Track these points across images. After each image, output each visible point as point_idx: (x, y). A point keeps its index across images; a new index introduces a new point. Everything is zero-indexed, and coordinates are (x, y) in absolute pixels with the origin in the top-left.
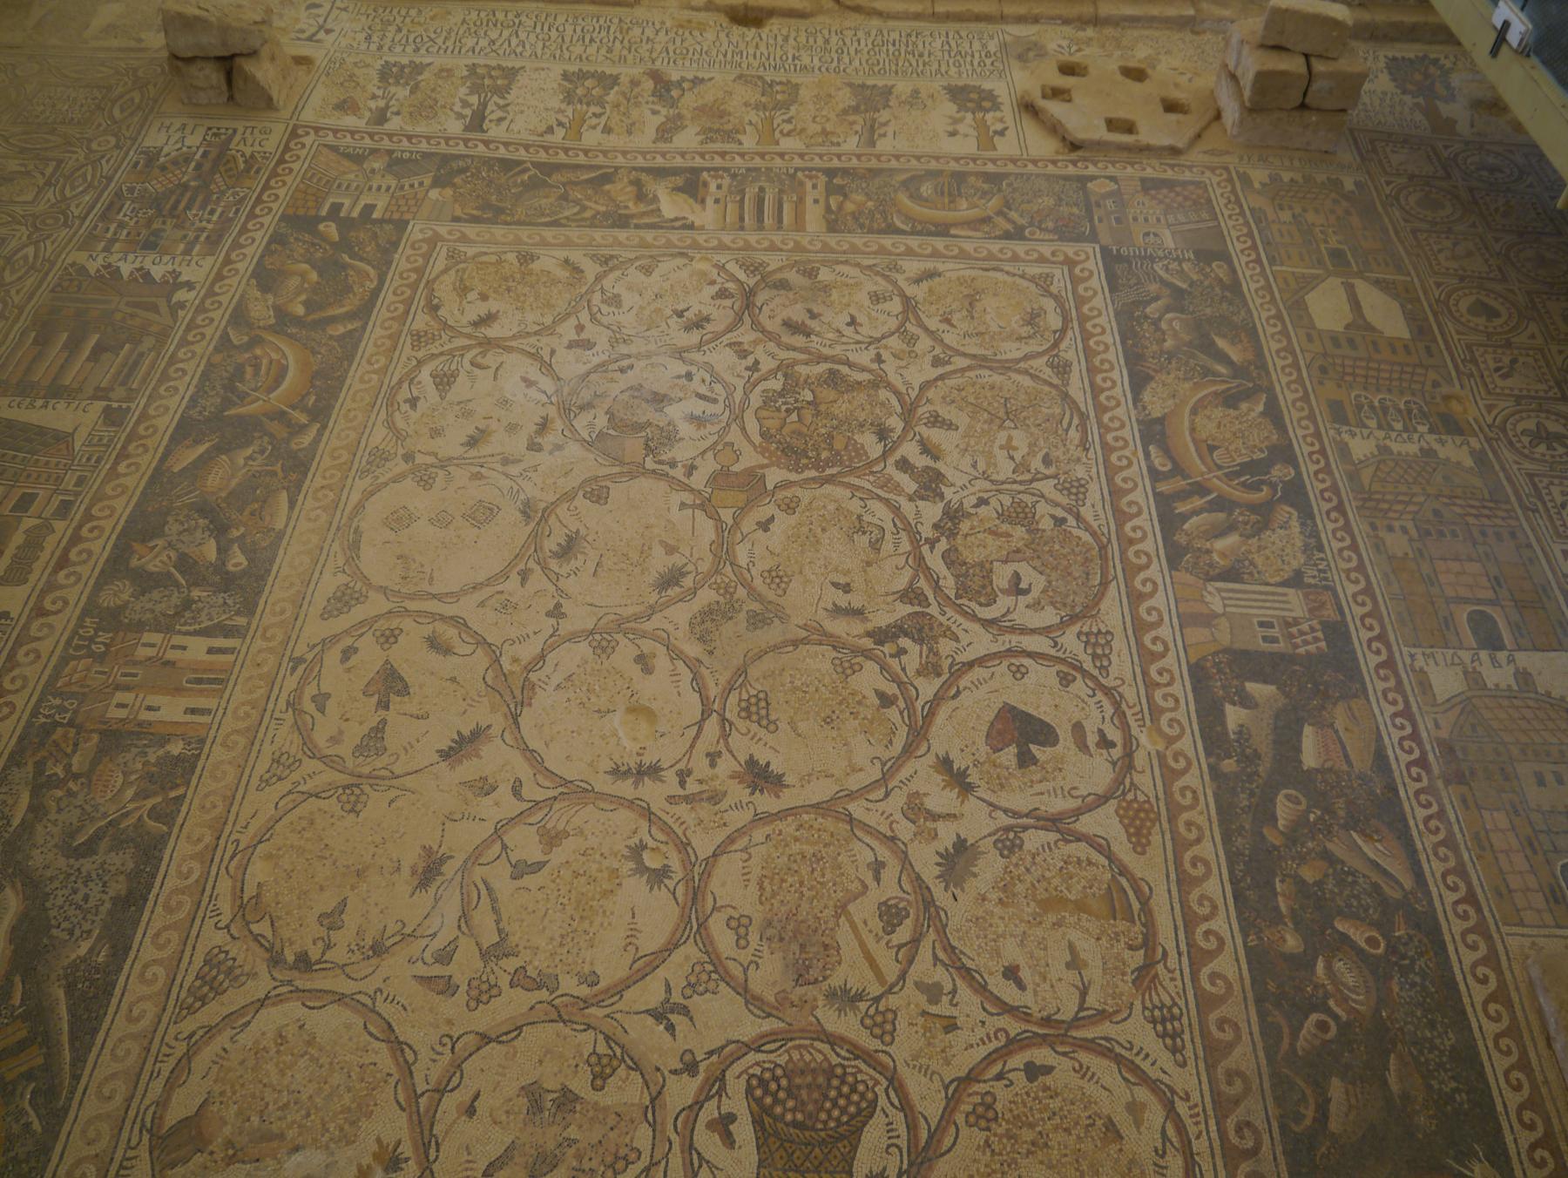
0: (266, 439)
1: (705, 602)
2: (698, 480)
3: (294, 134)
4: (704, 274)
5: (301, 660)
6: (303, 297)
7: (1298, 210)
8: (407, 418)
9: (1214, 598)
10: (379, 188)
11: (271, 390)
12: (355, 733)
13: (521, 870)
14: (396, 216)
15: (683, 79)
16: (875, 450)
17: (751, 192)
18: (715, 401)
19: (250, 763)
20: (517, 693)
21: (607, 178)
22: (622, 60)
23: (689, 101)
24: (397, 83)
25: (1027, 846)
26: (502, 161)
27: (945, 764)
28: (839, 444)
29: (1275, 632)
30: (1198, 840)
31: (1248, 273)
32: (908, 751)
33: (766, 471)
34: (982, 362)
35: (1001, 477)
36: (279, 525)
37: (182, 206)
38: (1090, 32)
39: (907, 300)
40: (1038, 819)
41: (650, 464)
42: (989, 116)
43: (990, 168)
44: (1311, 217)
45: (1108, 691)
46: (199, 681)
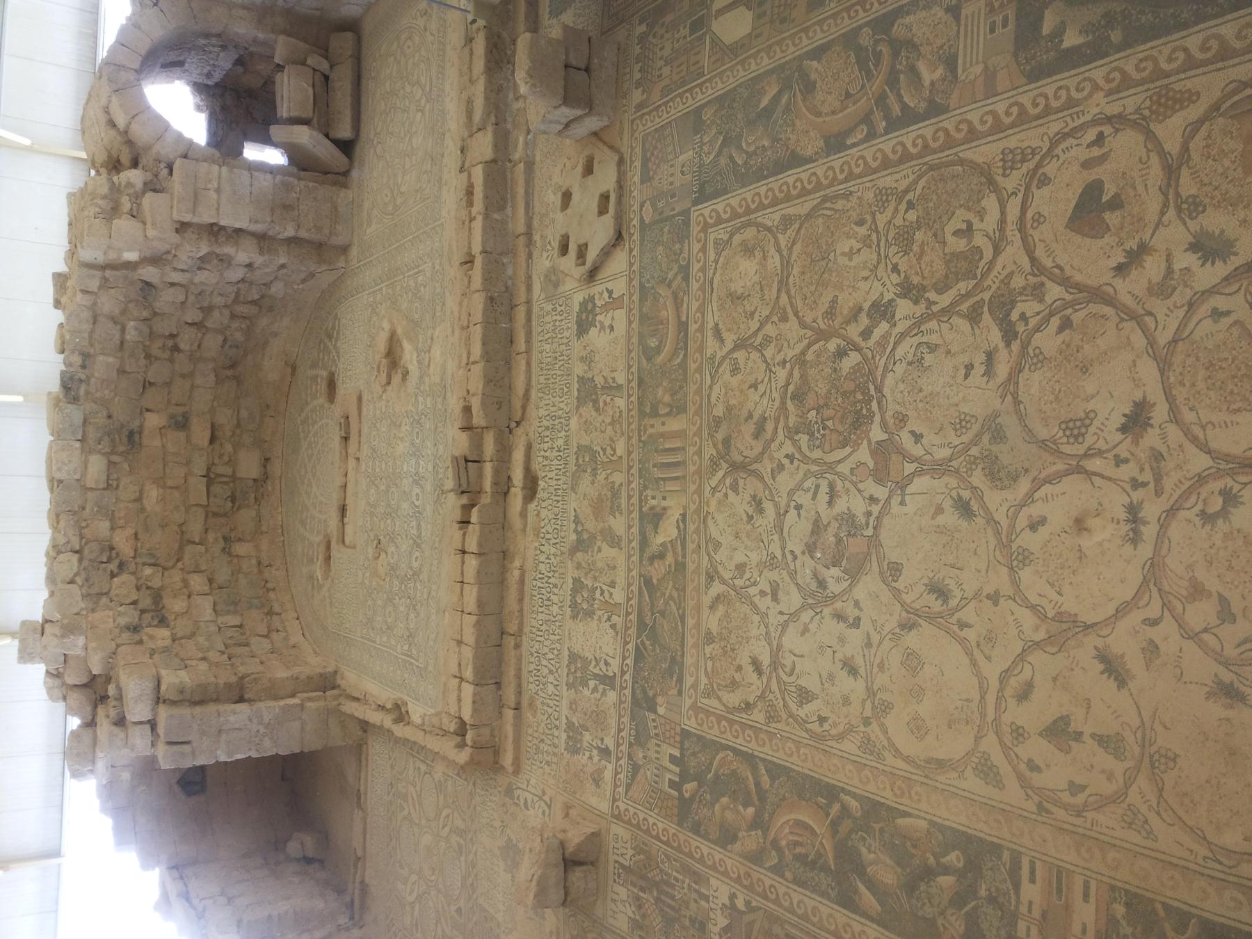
0: (853, 836)
1: (983, 479)
2: (881, 492)
3: (618, 817)
4: (719, 503)
5: (1040, 806)
6: (741, 808)
7: (662, 63)
8: (835, 725)
9: (970, 70)
10: (657, 752)
11: (813, 831)
12: (1106, 760)
13: (1226, 613)
14: (678, 738)
15: (575, 531)
16: (853, 358)
17: (658, 474)
18: (818, 487)
19: (1133, 847)
20: (1065, 626)
21: (648, 582)
22: (563, 576)
23: (591, 525)
24: (581, 741)
25: (1193, 191)
26: (636, 661)
27: (1120, 269)
28: (850, 386)
29: (999, 19)
30: (1186, 50)
31: (710, 92)
32: (1110, 301)
33: (874, 440)
34: (783, 284)
35: (875, 256)
36: (924, 824)
37: (673, 903)
38: (537, 237)
39: (736, 347)
40: (1169, 185)
41: (869, 532)
42: (599, 303)
43: (636, 298)
44: (667, 52)
45: (1054, 144)
46: (1059, 890)
